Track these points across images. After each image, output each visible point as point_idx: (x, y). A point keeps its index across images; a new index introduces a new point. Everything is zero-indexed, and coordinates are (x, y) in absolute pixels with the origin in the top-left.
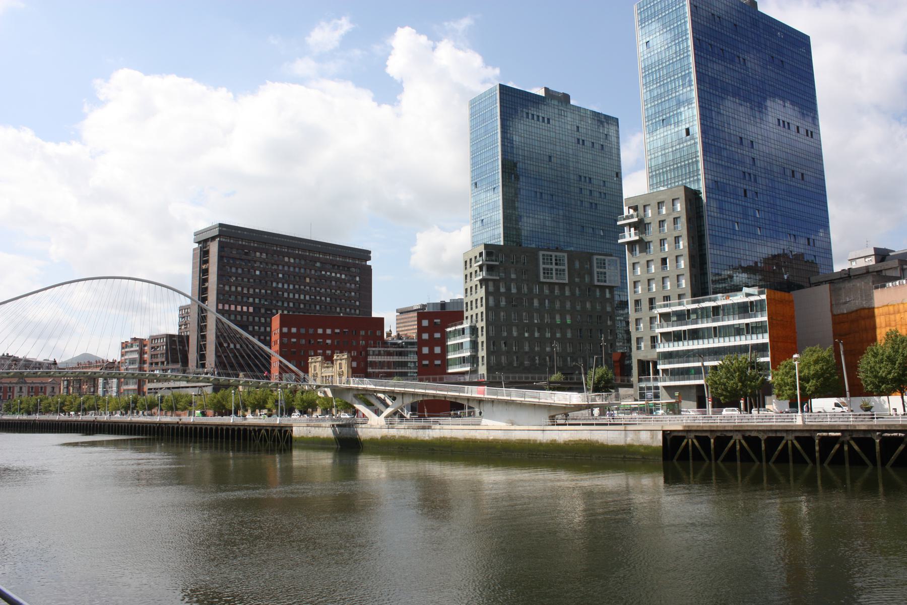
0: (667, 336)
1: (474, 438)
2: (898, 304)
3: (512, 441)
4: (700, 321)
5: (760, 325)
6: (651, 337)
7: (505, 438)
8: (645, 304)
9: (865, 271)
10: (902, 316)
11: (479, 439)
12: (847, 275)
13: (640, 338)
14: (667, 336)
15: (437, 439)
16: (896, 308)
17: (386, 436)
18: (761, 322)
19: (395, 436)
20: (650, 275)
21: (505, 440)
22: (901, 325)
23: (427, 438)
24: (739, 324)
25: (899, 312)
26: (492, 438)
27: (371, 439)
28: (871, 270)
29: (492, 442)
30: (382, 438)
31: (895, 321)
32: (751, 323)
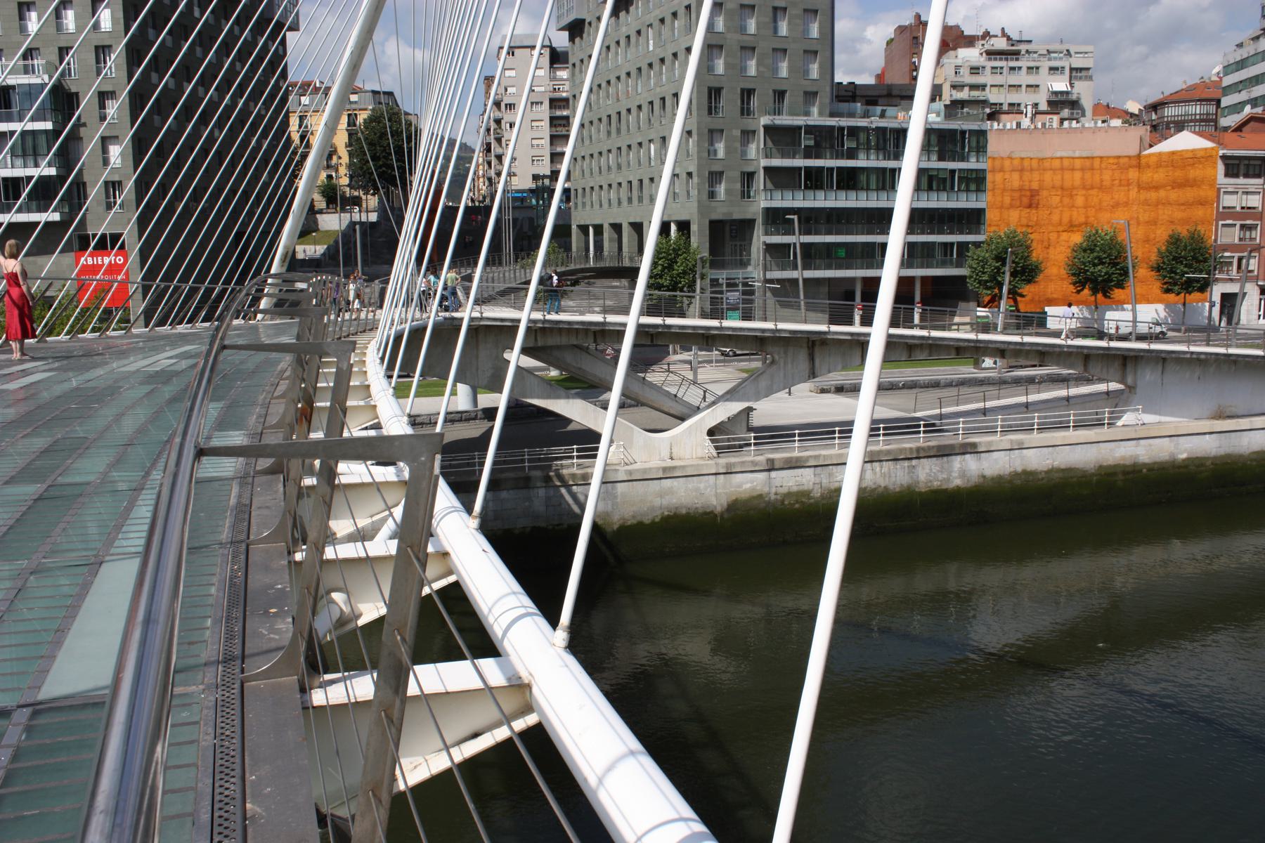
0: (780, 179)
1: (1122, 462)
2: (1002, 158)
3: (1241, 456)
4: (862, 155)
5: (974, 176)
6: (741, 172)
7: (1222, 452)
8: (730, 102)
9: (885, 92)
10: (1007, 176)
11: (1144, 465)
12: (850, 94)
13: (716, 173)
14: (780, 179)
15: (999, 480)
16: (997, 163)
17: (760, 496)
18: (976, 170)
19: (806, 494)
20: (745, 38)
21: (1222, 457)
22: (1004, 190)
23: (957, 482)
24: (938, 170)
25: (1002, 170)
26: (1184, 456)
27: (666, 519)
28: (895, 92)
29: (1186, 467)
30: (734, 506)
31: (994, 182)
32: (960, 170)
